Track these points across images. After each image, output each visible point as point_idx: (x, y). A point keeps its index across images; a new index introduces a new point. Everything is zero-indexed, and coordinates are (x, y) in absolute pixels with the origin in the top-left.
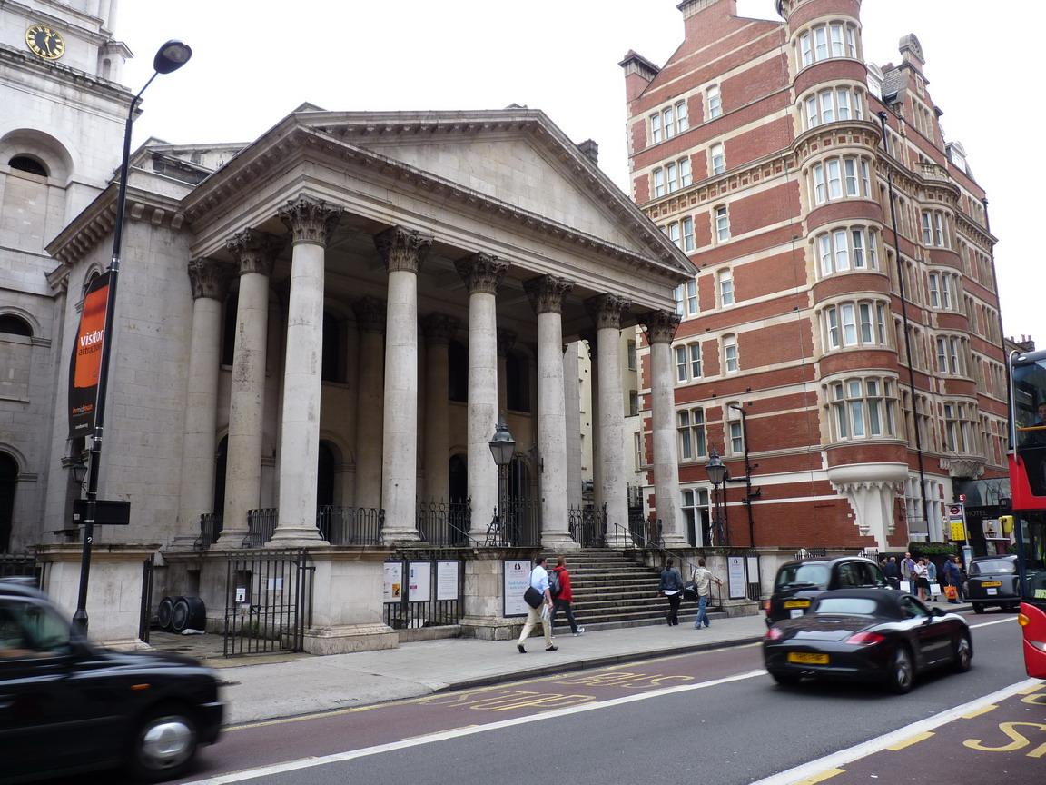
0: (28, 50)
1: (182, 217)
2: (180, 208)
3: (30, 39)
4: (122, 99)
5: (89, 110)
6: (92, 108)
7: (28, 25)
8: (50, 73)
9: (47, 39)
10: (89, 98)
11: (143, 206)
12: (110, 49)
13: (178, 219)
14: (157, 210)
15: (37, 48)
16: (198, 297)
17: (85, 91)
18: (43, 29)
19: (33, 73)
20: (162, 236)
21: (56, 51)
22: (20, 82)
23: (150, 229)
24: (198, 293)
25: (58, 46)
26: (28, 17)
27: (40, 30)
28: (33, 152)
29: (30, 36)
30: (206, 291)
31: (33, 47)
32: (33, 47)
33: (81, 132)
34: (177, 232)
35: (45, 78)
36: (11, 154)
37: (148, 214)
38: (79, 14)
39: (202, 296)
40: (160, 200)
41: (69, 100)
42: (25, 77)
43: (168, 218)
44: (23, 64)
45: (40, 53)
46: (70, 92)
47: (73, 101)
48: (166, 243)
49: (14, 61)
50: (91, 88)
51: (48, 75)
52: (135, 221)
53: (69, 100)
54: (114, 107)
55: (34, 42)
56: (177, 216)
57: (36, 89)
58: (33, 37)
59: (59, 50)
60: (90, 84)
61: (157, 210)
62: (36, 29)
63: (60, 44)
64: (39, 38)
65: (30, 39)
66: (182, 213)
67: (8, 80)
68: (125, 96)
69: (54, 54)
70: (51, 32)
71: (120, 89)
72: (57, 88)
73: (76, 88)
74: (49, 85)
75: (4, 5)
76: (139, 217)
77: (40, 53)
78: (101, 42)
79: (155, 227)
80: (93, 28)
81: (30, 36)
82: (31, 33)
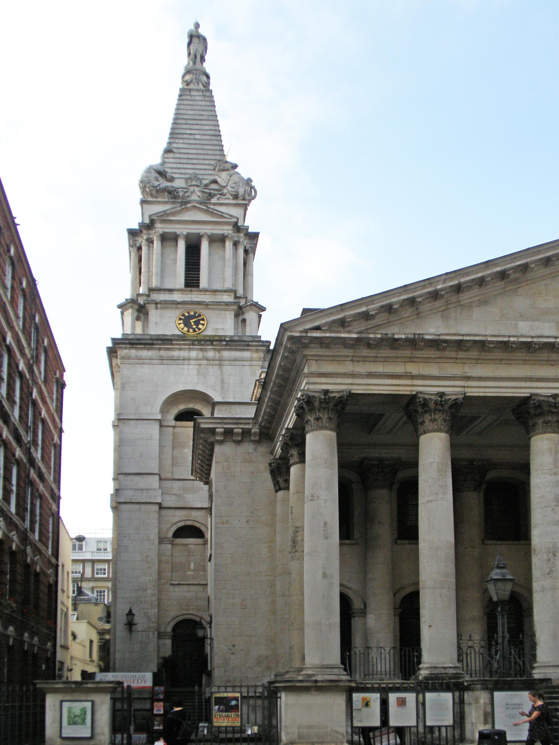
0: (180, 333)
4: (253, 346)
5: (226, 363)
6: (229, 360)
7: (178, 313)
8: (193, 344)
10: (226, 354)
12: (244, 310)
15: (186, 329)
17: (222, 349)
18: (189, 313)
21: (200, 326)
22: (172, 359)
25: (201, 322)
27: (187, 314)
31: (183, 329)
32: (183, 329)
33: (222, 381)
36: (175, 411)
38: (216, 291)
41: (210, 360)
42: (176, 353)
45: (188, 331)
46: (211, 354)
47: (213, 360)
50: (226, 345)
51: (191, 347)
53: (210, 360)
54: (247, 354)
57: (184, 359)
58: (181, 322)
59: (203, 325)
60: (224, 343)
62: (183, 315)
63: (203, 320)
64: (186, 321)
65: (180, 324)
68: (254, 344)
69: (199, 329)
71: (251, 339)
72: (201, 354)
73: (214, 349)
74: (193, 354)
75: (159, 306)
77: (188, 331)
78: (235, 307)
80: (228, 298)
82: (180, 319)
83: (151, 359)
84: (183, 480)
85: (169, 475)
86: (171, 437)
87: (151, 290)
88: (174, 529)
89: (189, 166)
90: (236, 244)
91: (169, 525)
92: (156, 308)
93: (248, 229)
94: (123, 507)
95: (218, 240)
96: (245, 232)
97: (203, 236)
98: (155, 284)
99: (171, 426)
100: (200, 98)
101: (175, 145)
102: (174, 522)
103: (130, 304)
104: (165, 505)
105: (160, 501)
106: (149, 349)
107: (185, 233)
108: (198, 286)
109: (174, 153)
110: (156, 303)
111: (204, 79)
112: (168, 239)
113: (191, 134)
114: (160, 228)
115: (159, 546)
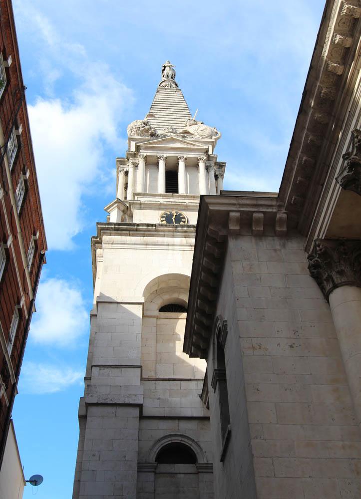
1: (285, 216)
2: (280, 206)
3: (162, 221)
9: (174, 217)
11: (238, 214)
13: (280, 218)
14: (255, 215)
16: (331, 291)
19: (164, 236)
20: (269, 245)
23: (253, 240)
24: (328, 287)
25: (183, 220)
26: (159, 209)
28: (175, 296)
29: (162, 219)
30: (337, 279)
34: (285, 236)
35: (173, 236)
37: (247, 221)
39: (336, 286)
40: (254, 202)
43: (270, 222)
44: (156, 231)
48: (275, 250)
49: (149, 231)
52: (237, 235)
55: (165, 221)
56: (278, 216)
58: (164, 219)
61: (255, 215)
66: (284, 211)
67: (147, 245)
70: (177, 213)
76: (237, 228)
79: (260, 236)
81: (162, 219)
82: (162, 217)
83: (135, 244)
84: (169, 380)
85: (152, 375)
86: (154, 329)
87: (135, 194)
88: (157, 449)
89: (166, 124)
90: (207, 168)
91: (151, 443)
92: (141, 209)
93: (216, 158)
94: (93, 410)
95: (193, 165)
96: (214, 160)
97: (180, 158)
98: (139, 190)
99: (154, 317)
100: (173, 93)
101: (155, 114)
102: (158, 437)
103: (116, 205)
104: (146, 412)
105: (140, 402)
106: (133, 235)
107: (165, 156)
108: (177, 192)
109: (155, 117)
110: (141, 204)
111: (174, 86)
112: (151, 163)
113: (167, 109)
114: (143, 153)
115: (138, 476)
